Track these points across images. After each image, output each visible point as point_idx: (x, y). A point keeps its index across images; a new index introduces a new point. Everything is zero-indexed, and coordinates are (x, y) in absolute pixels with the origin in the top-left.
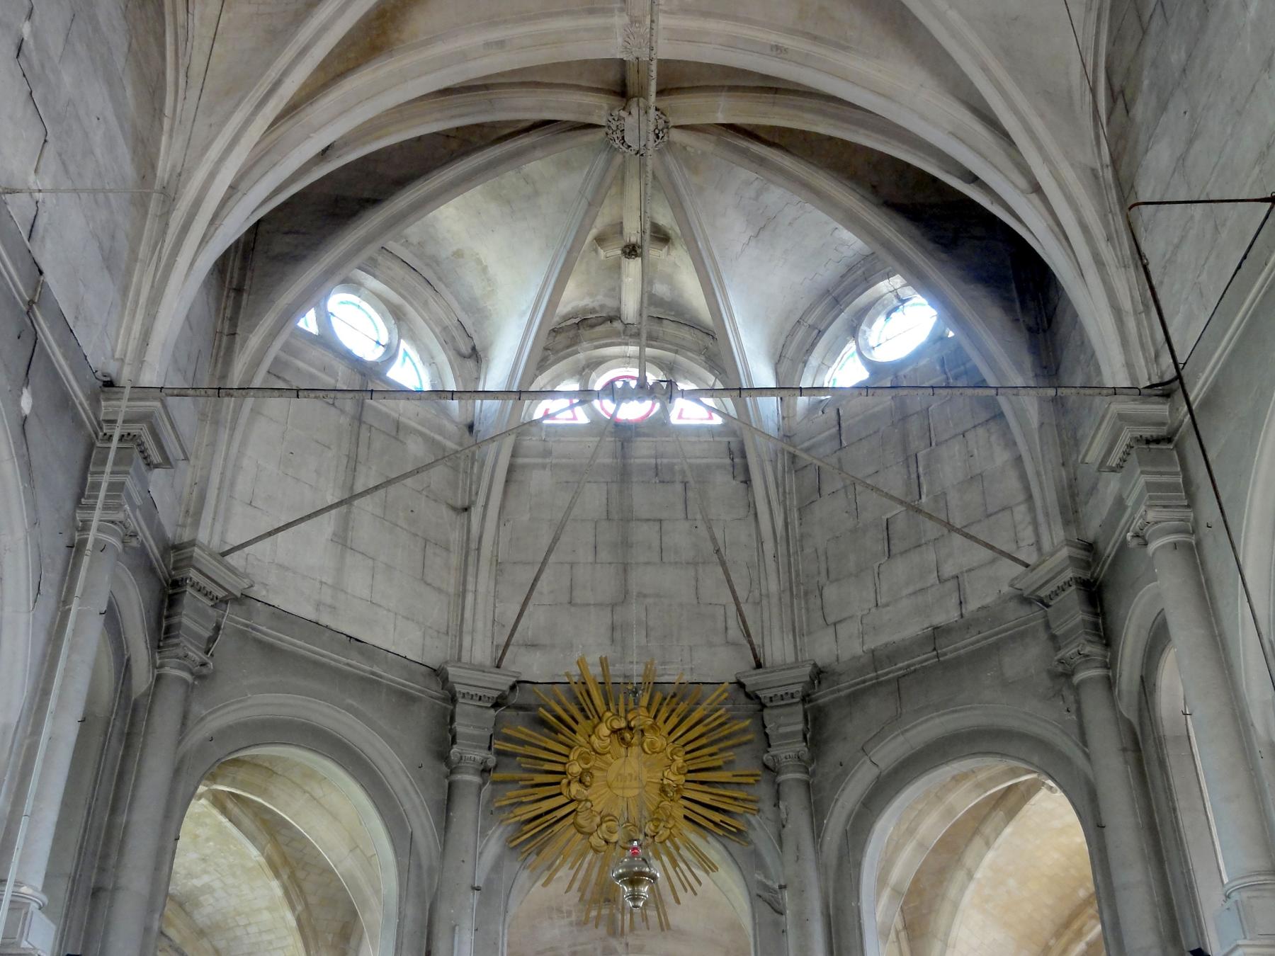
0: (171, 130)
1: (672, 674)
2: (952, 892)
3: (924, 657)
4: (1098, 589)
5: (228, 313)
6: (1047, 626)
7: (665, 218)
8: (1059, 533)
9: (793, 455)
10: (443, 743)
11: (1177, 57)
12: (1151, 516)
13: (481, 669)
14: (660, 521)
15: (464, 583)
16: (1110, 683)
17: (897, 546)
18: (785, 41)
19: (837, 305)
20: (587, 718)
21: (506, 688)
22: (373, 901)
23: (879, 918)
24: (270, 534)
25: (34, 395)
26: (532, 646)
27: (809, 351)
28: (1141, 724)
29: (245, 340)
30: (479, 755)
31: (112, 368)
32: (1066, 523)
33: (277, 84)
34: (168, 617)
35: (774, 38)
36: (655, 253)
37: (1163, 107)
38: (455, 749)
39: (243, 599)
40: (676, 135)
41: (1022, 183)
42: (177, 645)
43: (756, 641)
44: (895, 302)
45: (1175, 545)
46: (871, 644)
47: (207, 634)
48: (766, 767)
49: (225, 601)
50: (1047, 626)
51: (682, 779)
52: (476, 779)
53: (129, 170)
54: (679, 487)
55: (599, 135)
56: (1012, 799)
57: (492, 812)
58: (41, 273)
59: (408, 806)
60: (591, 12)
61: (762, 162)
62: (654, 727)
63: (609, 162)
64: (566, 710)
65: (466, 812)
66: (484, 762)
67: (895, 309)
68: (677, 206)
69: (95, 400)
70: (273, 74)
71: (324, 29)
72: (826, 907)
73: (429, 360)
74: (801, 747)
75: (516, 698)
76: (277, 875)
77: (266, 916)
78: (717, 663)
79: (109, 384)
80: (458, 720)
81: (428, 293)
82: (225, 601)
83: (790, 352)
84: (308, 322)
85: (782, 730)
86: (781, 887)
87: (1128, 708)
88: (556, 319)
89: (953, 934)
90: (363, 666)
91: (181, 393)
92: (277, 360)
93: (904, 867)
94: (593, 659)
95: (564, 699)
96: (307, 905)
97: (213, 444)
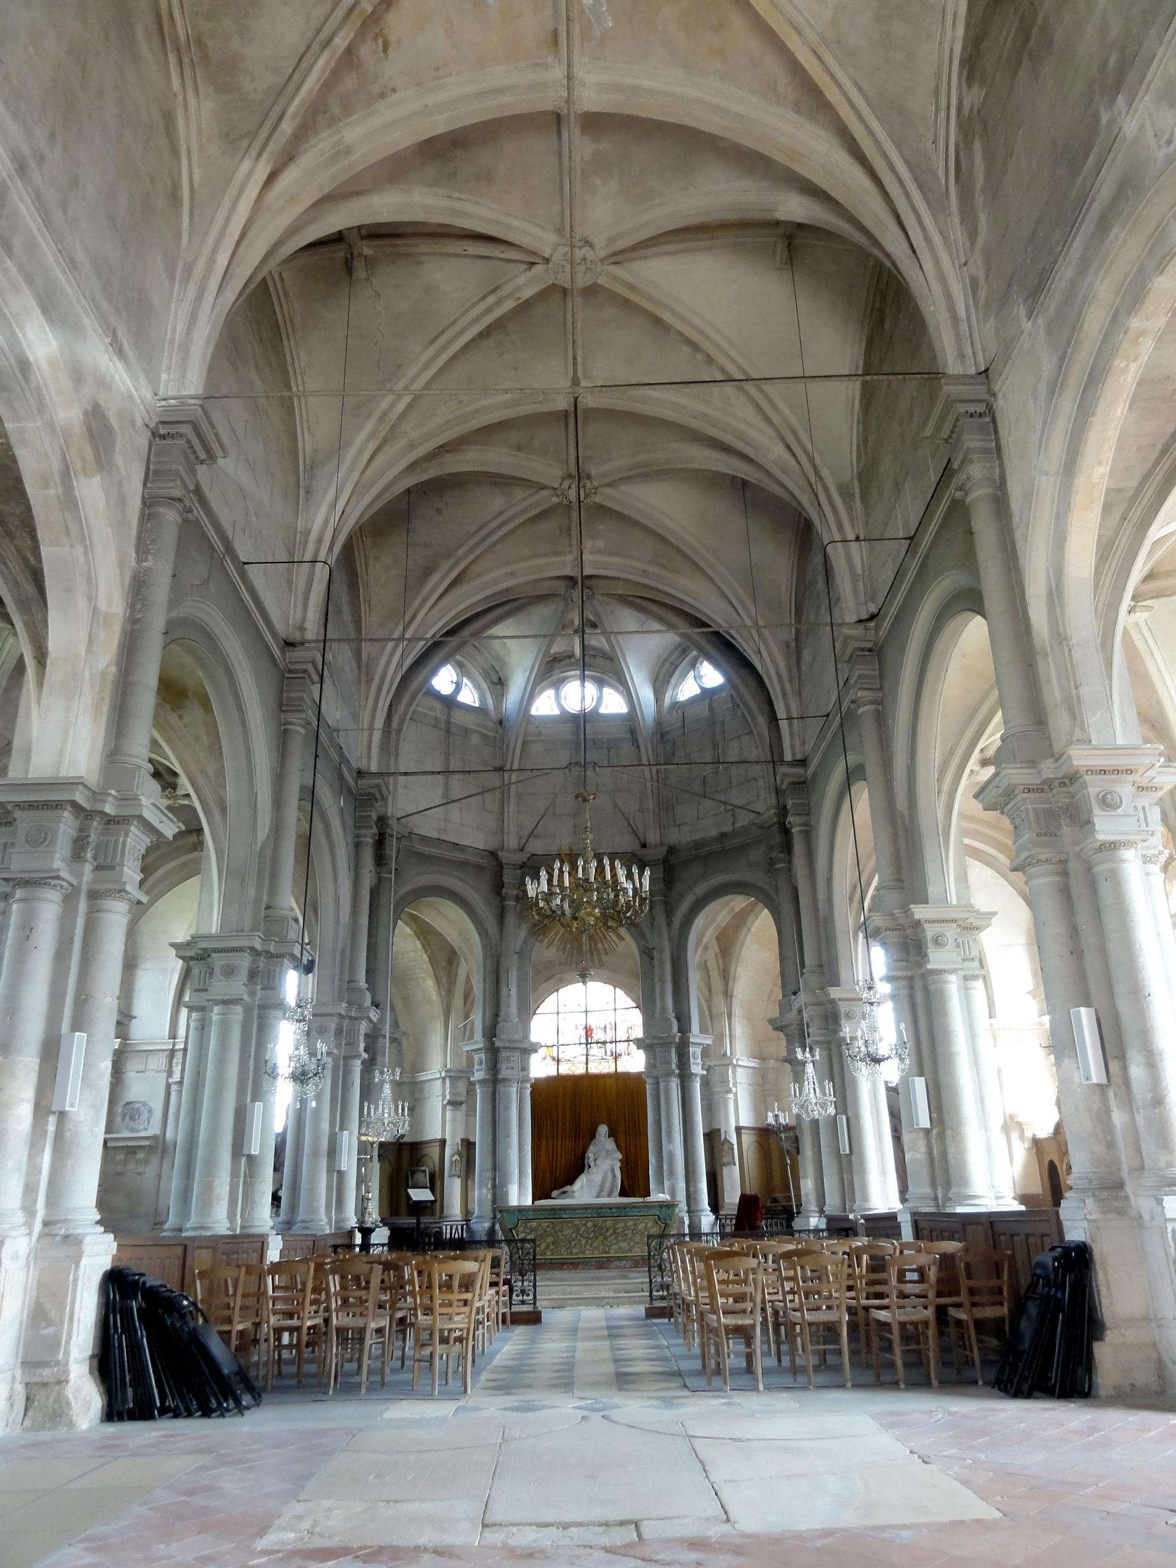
2: (742, 936)
3: (716, 847)
9: (661, 731)
18: (649, 568)
23: (697, 959)
35: (643, 566)
45: (800, 832)
46: (698, 836)
54: (605, 751)
60: (556, 554)
65: (511, 919)
66: (517, 896)
72: (672, 957)
73: (477, 687)
75: (530, 864)
77: (412, 954)
80: (505, 876)
96: (432, 952)
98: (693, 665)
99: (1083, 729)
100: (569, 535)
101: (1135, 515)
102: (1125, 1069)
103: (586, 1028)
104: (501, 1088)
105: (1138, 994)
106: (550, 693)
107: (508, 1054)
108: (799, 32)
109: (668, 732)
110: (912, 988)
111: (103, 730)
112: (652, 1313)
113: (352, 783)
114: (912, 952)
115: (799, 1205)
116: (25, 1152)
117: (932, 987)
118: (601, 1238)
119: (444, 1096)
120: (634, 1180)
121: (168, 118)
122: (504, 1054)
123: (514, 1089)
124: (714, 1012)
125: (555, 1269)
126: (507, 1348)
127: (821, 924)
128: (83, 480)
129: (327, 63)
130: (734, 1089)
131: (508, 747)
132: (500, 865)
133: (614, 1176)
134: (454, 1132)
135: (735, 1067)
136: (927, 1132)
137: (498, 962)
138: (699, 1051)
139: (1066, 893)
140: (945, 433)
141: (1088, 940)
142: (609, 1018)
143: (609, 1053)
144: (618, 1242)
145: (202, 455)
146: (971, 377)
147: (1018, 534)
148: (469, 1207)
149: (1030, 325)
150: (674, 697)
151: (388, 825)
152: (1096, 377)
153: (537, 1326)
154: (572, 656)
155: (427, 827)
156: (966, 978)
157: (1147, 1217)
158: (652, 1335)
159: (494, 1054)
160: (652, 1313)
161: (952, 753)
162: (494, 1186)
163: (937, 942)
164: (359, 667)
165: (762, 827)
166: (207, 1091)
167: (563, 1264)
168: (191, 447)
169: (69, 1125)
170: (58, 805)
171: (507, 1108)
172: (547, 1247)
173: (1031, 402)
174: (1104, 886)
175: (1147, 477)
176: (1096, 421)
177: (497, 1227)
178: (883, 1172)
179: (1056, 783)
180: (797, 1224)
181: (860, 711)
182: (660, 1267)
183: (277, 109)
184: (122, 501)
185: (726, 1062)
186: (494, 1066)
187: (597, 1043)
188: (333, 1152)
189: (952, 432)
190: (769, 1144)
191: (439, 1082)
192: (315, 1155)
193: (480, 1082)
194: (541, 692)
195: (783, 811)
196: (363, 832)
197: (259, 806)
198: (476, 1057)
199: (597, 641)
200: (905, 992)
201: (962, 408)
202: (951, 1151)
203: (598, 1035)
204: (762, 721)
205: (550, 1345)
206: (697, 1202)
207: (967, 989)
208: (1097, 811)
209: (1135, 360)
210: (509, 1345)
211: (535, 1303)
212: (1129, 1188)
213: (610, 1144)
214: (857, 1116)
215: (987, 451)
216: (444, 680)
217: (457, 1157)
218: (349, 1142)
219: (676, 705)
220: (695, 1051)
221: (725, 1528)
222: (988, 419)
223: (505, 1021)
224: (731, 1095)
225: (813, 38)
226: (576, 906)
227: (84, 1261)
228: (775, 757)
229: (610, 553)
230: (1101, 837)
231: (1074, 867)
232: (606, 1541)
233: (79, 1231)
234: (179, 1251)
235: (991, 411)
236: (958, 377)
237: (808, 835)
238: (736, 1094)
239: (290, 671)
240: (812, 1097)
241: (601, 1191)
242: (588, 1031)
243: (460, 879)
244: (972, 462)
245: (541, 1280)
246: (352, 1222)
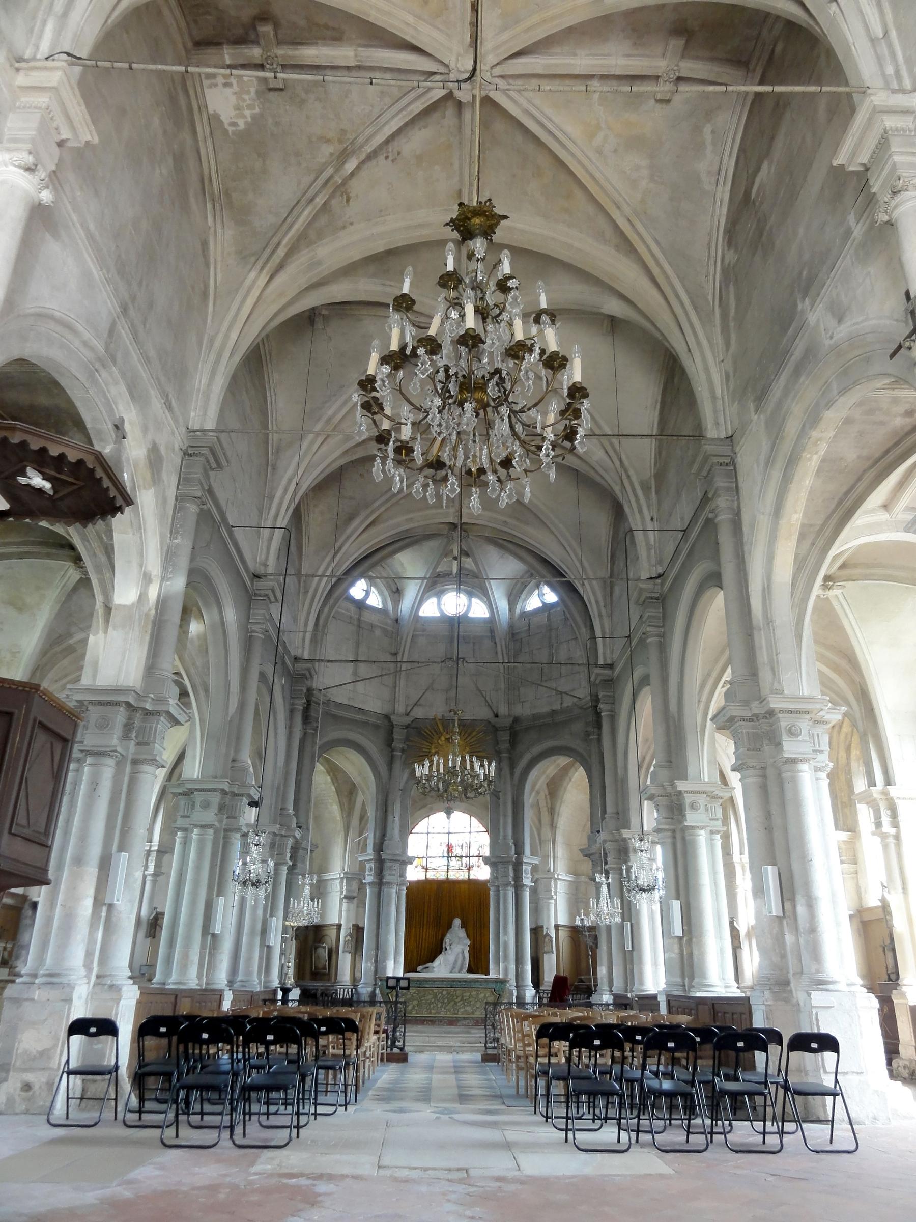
9: (513, 633)
10: (389, 742)
18: (508, 520)
27: (521, 593)
30: (401, 746)
35: (504, 519)
45: (607, 716)
54: (472, 645)
65: (397, 765)
72: (513, 799)
73: (381, 593)
75: (413, 725)
78: (483, 713)
83: (514, 592)
98: (538, 586)
99: (779, 682)
101: (820, 543)
102: (794, 907)
104: (385, 889)
105: (805, 860)
106: (434, 600)
108: (619, 208)
110: (674, 837)
111: (145, 652)
112: (486, 1058)
113: (290, 666)
114: (676, 812)
115: (596, 986)
116: (87, 930)
117: (687, 838)
119: (342, 892)
120: (478, 961)
121: (205, 244)
122: (387, 864)
124: (543, 838)
125: (418, 1024)
126: (385, 1077)
128: (143, 491)
129: (310, 213)
131: (401, 639)
132: (392, 725)
133: (464, 958)
136: (680, 938)
137: (387, 796)
138: (529, 868)
139: (764, 789)
140: (704, 473)
141: (777, 821)
142: (465, 838)
143: (464, 865)
145: (214, 465)
146: (721, 440)
147: (746, 548)
148: (357, 975)
149: (756, 417)
151: (313, 695)
152: (792, 461)
155: (340, 697)
156: (712, 832)
157: (802, 1005)
158: (485, 1073)
159: (380, 864)
160: (486, 1058)
161: (709, 675)
162: (376, 961)
163: (693, 807)
164: (299, 583)
165: (581, 708)
166: (187, 888)
168: (208, 462)
169: (115, 913)
170: (117, 704)
171: (389, 904)
172: (414, 1007)
173: (755, 466)
174: (788, 787)
175: (829, 518)
176: (793, 487)
177: (378, 991)
178: (655, 964)
179: (761, 716)
180: (594, 999)
181: (648, 641)
182: (493, 1025)
183: (275, 240)
184: (165, 500)
185: (550, 876)
188: (264, 932)
189: (708, 473)
193: (371, 884)
195: (596, 700)
196: (297, 701)
197: (231, 690)
198: (368, 866)
199: (468, 563)
200: (669, 840)
201: (715, 460)
202: (695, 952)
203: (457, 851)
204: (584, 632)
205: (414, 1076)
206: (523, 980)
207: (712, 840)
208: (785, 737)
209: (816, 453)
210: (387, 1075)
212: (792, 985)
213: (462, 933)
214: (638, 923)
215: (729, 489)
216: (358, 590)
217: (349, 938)
218: (276, 924)
219: (524, 614)
220: (526, 868)
221: (517, 1173)
222: (732, 468)
223: (390, 840)
224: (552, 901)
225: (627, 210)
226: (447, 784)
227: (122, 1002)
228: (592, 663)
230: (786, 755)
231: (770, 772)
232: (450, 1177)
233: (119, 982)
234: (172, 998)
235: (733, 463)
236: (713, 439)
237: (613, 718)
239: (256, 595)
240: (605, 910)
241: (454, 968)
242: (450, 848)
243: (362, 734)
244: (719, 496)
245: (409, 1032)
246: (276, 983)
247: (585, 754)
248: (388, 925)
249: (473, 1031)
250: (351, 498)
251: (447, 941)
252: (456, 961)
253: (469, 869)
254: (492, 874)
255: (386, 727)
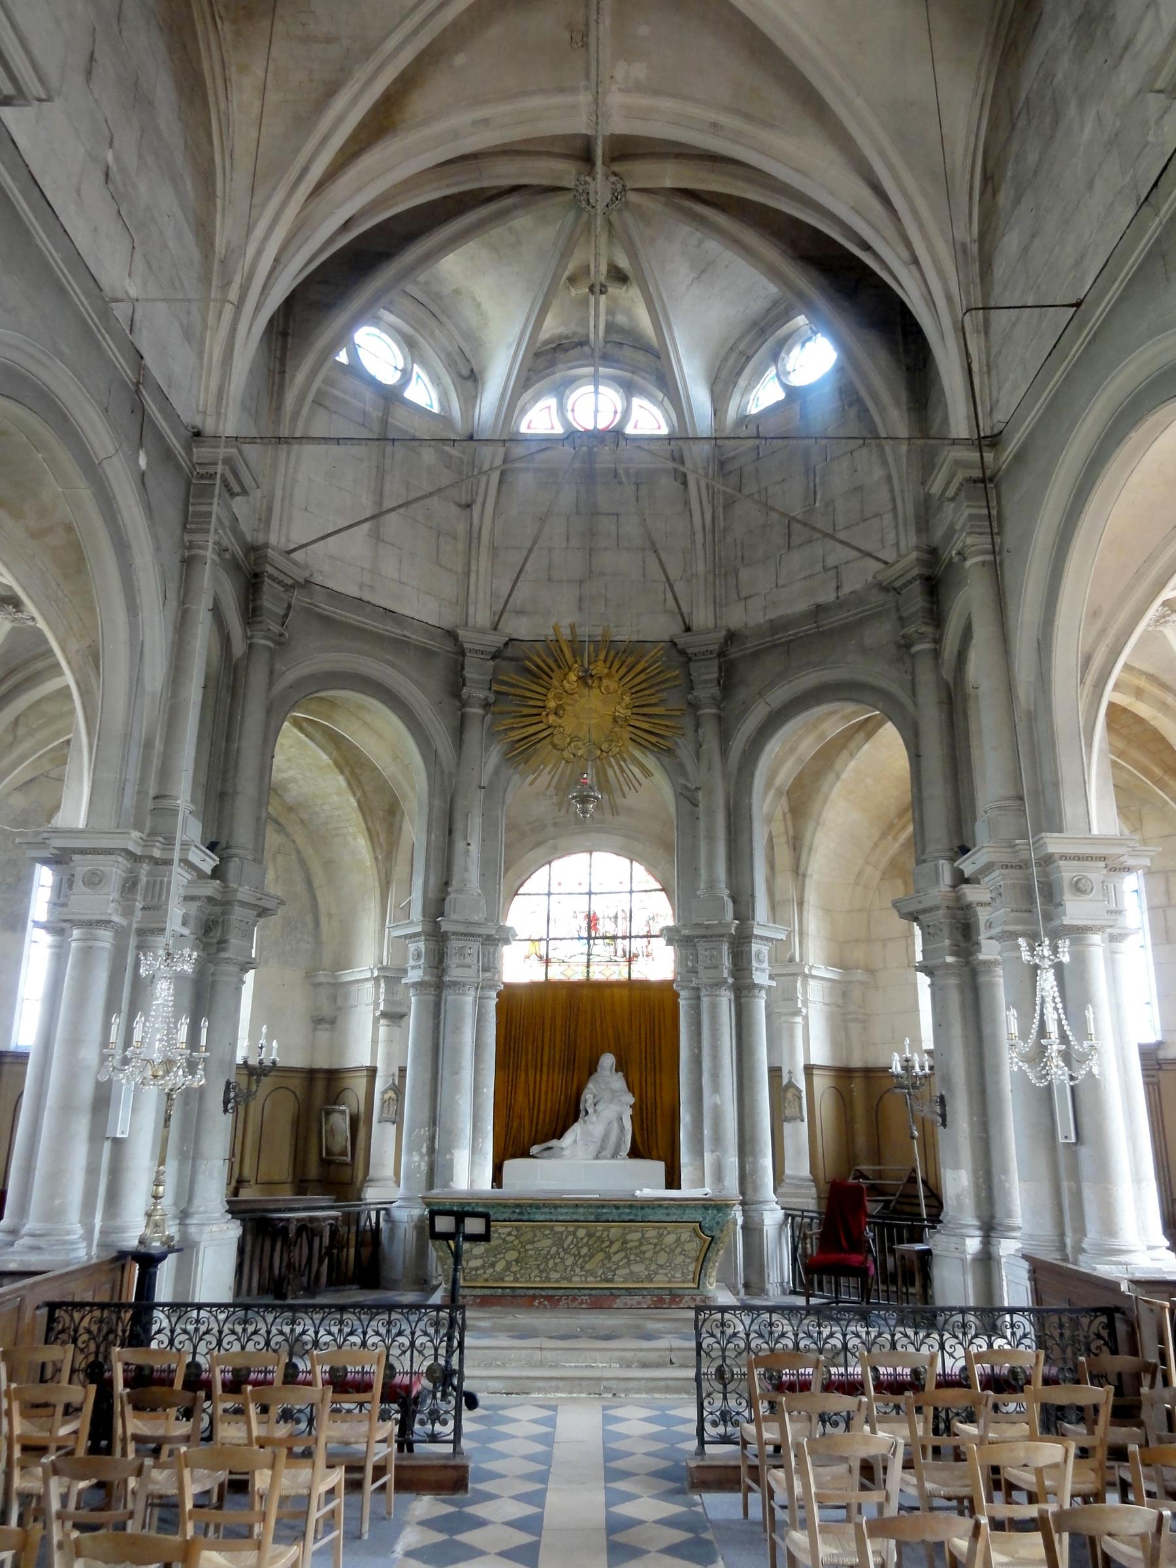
0: (223, 209)
1: (624, 634)
3: (808, 627)
4: (935, 582)
5: (278, 354)
6: (898, 609)
7: (623, 263)
8: (913, 540)
10: (456, 686)
11: (1032, 158)
12: (969, 541)
13: (482, 631)
14: (618, 515)
15: (469, 566)
16: (936, 654)
17: (796, 540)
18: (723, 119)
19: (760, 338)
20: (560, 667)
21: (501, 645)
22: (411, 794)
23: (765, 809)
24: (323, 538)
25: (147, 454)
26: (521, 612)
28: (955, 684)
29: (293, 377)
30: (481, 694)
31: (198, 421)
32: (919, 531)
33: (305, 170)
34: (254, 600)
35: (712, 116)
36: (613, 290)
37: (1017, 201)
38: (465, 690)
39: (307, 584)
40: (632, 197)
41: (905, 255)
42: (261, 622)
43: (685, 610)
44: (809, 332)
45: (984, 563)
46: (772, 615)
47: (282, 613)
48: (690, 704)
49: (293, 587)
50: (898, 609)
51: (629, 712)
52: (480, 711)
53: (196, 254)
55: (569, 196)
56: (870, 725)
57: (492, 735)
58: (142, 358)
59: (432, 731)
60: (562, 90)
61: (702, 221)
62: (609, 676)
63: (578, 218)
64: (544, 661)
65: (474, 735)
66: (486, 699)
67: (810, 339)
68: (633, 256)
69: (188, 449)
70: (301, 160)
71: (340, 119)
73: (436, 381)
74: (715, 691)
75: (509, 652)
76: (342, 772)
77: (335, 798)
78: (658, 627)
79: (198, 434)
80: (467, 668)
81: (433, 323)
82: (293, 587)
83: (723, 375)
84: (343, 357)
85: (702, 678)
86: (698, 789)
87: (947, 673)
88: (538, 345)
89: (824, 814)
90: (397, 631)
91: (252, 440)
92: (319, 391)
93: (786, 775)
94: (565, 622)
95: (543, 654)
96: (364, 792)
97: (274, 466)
100: (586, 45)
103: (588, 916)
104: (449, 996)
106: (551, 401)
107: (461, 944)
109: (734, 458)
118: (601, 1255)
120: (654, 1137)
122: (454, 944)
123: (469, 1000)
124: (778, 897)
125: (519, 1306)
127: (1021, 727)
130: (804, 1011)
133: (622, 1129)
134: (389, 1056)
135: (806, 977)
137: (452, 800)
142: (623, 902)
143: (620, 953)
144: (628, 1264)
150: (742, 407)
153: (458, 1497)
154: (583, 343)
159: (439, 942)
162: (431, 1150)
167: (534, 1297)
171: (457, 1030)
172: (509, 1265)
178: (1138, 1180)
186: (438, 960)
187: (604, 938)
188: (103, 1101)
190: (851, 1091)
191: (369, 985)
192: (67, 1107)
193: (414, 985)
194: (536, 399)
196: (198, 538)
206: (756, 1189)
211: (456, 1441)
213: (618, 1082)
217: (391, 1094)
219: (744, 420)
223: (459, 891)
224: (799, 1019)
229: (657, 92)
237: (996, 569)
238: (806, 1018)
242: (592, 921)
243: (393, 665)
247: (894, 688)
248: (456, 1072)
249: (652, 1325)
250: (329, 40)
251: (588, 1097)
252: (606, 1136)
253: (630, 961)
254: (681, 961)
255: (448, 657)
